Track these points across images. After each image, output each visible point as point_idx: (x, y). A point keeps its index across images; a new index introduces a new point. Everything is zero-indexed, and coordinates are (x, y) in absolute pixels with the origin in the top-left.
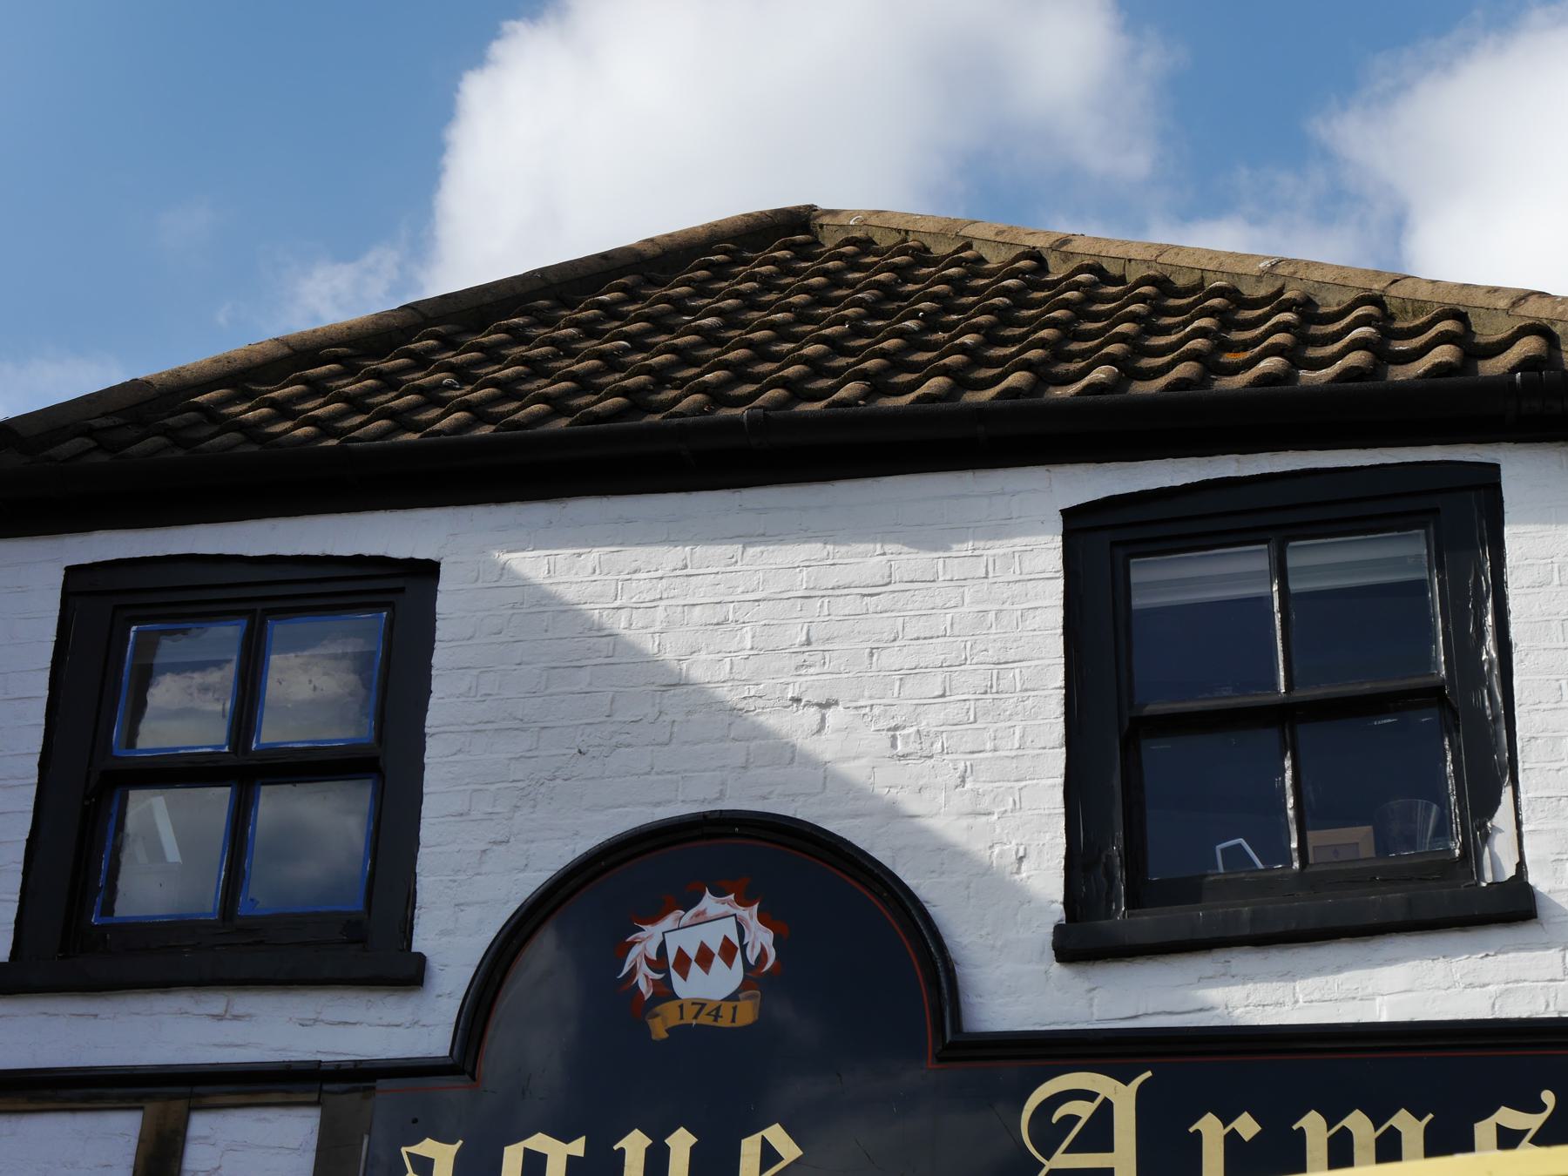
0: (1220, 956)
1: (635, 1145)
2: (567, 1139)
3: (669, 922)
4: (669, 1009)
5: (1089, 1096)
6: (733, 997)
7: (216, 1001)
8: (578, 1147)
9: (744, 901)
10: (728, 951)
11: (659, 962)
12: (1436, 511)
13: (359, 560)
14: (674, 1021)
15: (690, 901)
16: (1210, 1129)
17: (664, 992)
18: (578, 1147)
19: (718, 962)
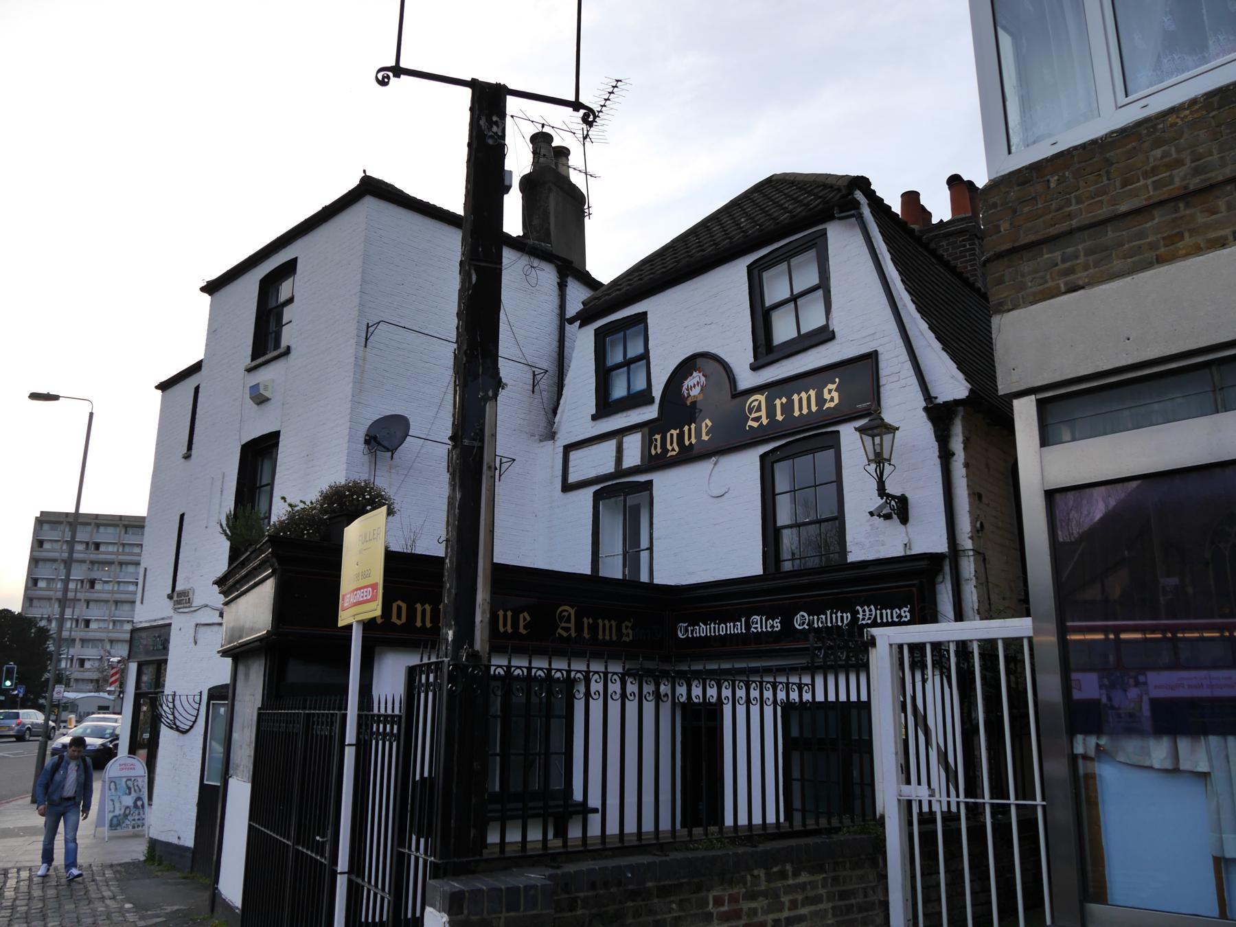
0: (780, 362)
1: (686, 428)
2: (676, 430)
3: (688, 380)
4: (690, 398)
5: (757, 400)
6: (699, 393)
7: (625, 414)
8: (678, 431)
9: (700, 372)
10: (698, 383)
11: (688, 390)
12: (816, 243)
13: (635, 314)
14: (690, 401)
15: (691, 375)
16: (778, 402)
17: (689, 395)
18: (678, 431)
19: (692, 386)
